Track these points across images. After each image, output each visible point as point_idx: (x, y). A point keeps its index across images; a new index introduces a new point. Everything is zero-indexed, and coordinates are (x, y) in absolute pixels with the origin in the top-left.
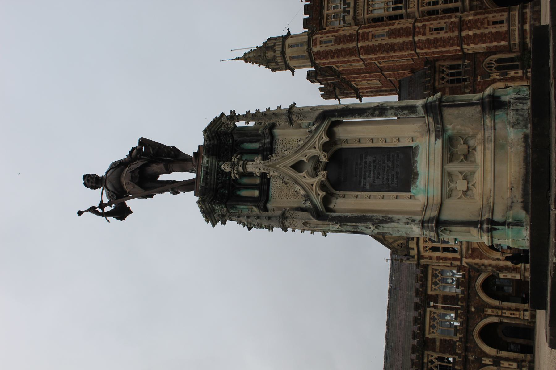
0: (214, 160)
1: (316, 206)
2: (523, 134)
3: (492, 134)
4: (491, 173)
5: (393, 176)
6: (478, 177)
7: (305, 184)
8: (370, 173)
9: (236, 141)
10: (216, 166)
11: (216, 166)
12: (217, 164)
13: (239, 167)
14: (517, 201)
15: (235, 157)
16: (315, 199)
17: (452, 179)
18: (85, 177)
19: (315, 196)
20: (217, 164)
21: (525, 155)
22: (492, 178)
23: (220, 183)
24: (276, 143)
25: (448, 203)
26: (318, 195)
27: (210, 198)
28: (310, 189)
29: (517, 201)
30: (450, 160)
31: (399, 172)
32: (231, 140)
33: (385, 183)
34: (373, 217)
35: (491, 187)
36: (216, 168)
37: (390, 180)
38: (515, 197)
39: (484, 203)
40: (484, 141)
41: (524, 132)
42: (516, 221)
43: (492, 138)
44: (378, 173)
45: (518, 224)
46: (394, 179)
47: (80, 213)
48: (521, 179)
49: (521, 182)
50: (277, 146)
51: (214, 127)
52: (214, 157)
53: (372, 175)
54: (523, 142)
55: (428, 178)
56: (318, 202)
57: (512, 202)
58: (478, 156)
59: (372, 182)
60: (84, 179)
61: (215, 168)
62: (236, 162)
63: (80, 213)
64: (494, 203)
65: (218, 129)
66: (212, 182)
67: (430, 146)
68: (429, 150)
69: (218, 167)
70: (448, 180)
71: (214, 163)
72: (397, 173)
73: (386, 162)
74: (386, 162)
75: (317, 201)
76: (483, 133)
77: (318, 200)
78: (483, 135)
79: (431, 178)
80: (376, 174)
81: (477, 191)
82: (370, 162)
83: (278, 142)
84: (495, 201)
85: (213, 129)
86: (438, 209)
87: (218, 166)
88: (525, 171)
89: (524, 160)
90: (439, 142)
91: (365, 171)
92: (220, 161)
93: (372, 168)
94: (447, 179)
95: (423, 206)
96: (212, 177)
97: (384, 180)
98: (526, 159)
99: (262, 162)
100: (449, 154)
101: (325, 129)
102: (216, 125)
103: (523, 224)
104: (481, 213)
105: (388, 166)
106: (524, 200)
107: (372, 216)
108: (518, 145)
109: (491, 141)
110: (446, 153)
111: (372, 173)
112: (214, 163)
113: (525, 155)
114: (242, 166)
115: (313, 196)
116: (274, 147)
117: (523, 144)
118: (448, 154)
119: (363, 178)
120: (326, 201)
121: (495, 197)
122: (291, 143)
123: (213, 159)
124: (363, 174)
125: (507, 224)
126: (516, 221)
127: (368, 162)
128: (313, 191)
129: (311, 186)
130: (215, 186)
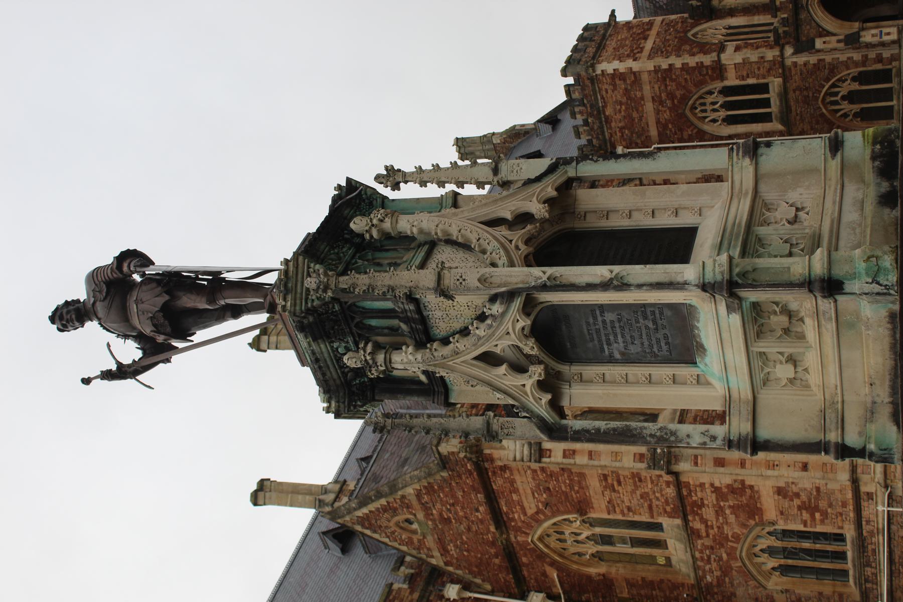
0: (322, 346)
1: (542, 417)
2: (887, 312)
3: (831, 309)
4: (835, 365)
5: (658, 341)
6: (811, 359)
7: (511, 389)
8: (616, 336)
9: (346, 303)
10: (330, 351)
11: (330, 351)
12: (329, 348)
13: (379, 367)
14: (883, 402)
15: (365, 351)
16: (537, 408)
17: (767, 358)
18: (52, 319)
19: (535, 403)
20: (329, 348)
21: (893, 341)
22: (837, 370)
23: (348, 372)
24: (428, 309)
25: (767, 397)
26: (539, 400)
27: (344, 403)
28: (521, 393)
29: (883, 402)
30: (759, 335)
31: (669, 335)
32: (335, 304)
33: (647, 351)
34: (644, 431)
35: (838, 437)
36: (332, 354)
37: (655, 346)
38: (878, 395)
39: (826, 398)
40: (817, 315)
41: (890, 309)
42: (881, 450)
43: (831, 315)
44: (631, 337)
45: (885, 458)
46: (663, 344)
47: (86, 381)
48: (887, 373)
49: (888, 377)
50: (430, 313)
51: (298, 302)
52: (320, 341)
53: (620, 339)
54: (888, 323)
55: (725, 363)
56: (544, 412)
57: (874, 403)
58: (809, 328)
59: (623, 350)
60: (53, 322)
61: (330, 354)
62: (371, 362)
63: (86, 381)
64: (843, 402)
65: (306, 303)
66: (335, 376)
67: (720, 319)
68: (718, 323)
69: (333, 351)
70: (760, 364)
71: (324, 349)
72: (666, 337)
73: (641, 320)
74: (641, 320)
75: (540, 411)
76: (814, 303)
77: (542, 408)
78: (815, 306)
79: (730, 364)
80: (628, 337)
81: (814, 379)
82: (612, 322)
83: (430, 307)
84: (845, 398)
85: (298, 308)
86: (750, 417)
87: (332, 350)
88: (893, 362)
89: (891, 348)
90: (735, 319)
91: (607, 335)
92: (333, 342)
93: (618, 330)
94: (757, 363)
95: (723, 400)
96: (332, 369)
97: (645, 346)
98: (893, 347)
99: (419, 356)
100: (755, 327)
101: (518, 310)
102: (298, 295)
103: (893, 458)
104: (823, 422)
105: (647, 327)
106: (893, 401)
107: (641, 428)
108: (880, 326)
109: (830, 319)
110: (751, 328)
111: (619, 336)
112: (324, 349)
113: (893, 341)
114: (383, 365)
115: (531, 405)
116: (425, 313)
117: (889, 326)
118: (754, 328)
119: (605, 343)
120: (556, 405)
121: (845, 393)
122: (455, 308)
123: (319, 345)
124: (604, 338)
125: (867, 454)
126: (881, 450)
127: (608, 321)
128: (528, 396)
129: (522, 387)
130: (342, 379)
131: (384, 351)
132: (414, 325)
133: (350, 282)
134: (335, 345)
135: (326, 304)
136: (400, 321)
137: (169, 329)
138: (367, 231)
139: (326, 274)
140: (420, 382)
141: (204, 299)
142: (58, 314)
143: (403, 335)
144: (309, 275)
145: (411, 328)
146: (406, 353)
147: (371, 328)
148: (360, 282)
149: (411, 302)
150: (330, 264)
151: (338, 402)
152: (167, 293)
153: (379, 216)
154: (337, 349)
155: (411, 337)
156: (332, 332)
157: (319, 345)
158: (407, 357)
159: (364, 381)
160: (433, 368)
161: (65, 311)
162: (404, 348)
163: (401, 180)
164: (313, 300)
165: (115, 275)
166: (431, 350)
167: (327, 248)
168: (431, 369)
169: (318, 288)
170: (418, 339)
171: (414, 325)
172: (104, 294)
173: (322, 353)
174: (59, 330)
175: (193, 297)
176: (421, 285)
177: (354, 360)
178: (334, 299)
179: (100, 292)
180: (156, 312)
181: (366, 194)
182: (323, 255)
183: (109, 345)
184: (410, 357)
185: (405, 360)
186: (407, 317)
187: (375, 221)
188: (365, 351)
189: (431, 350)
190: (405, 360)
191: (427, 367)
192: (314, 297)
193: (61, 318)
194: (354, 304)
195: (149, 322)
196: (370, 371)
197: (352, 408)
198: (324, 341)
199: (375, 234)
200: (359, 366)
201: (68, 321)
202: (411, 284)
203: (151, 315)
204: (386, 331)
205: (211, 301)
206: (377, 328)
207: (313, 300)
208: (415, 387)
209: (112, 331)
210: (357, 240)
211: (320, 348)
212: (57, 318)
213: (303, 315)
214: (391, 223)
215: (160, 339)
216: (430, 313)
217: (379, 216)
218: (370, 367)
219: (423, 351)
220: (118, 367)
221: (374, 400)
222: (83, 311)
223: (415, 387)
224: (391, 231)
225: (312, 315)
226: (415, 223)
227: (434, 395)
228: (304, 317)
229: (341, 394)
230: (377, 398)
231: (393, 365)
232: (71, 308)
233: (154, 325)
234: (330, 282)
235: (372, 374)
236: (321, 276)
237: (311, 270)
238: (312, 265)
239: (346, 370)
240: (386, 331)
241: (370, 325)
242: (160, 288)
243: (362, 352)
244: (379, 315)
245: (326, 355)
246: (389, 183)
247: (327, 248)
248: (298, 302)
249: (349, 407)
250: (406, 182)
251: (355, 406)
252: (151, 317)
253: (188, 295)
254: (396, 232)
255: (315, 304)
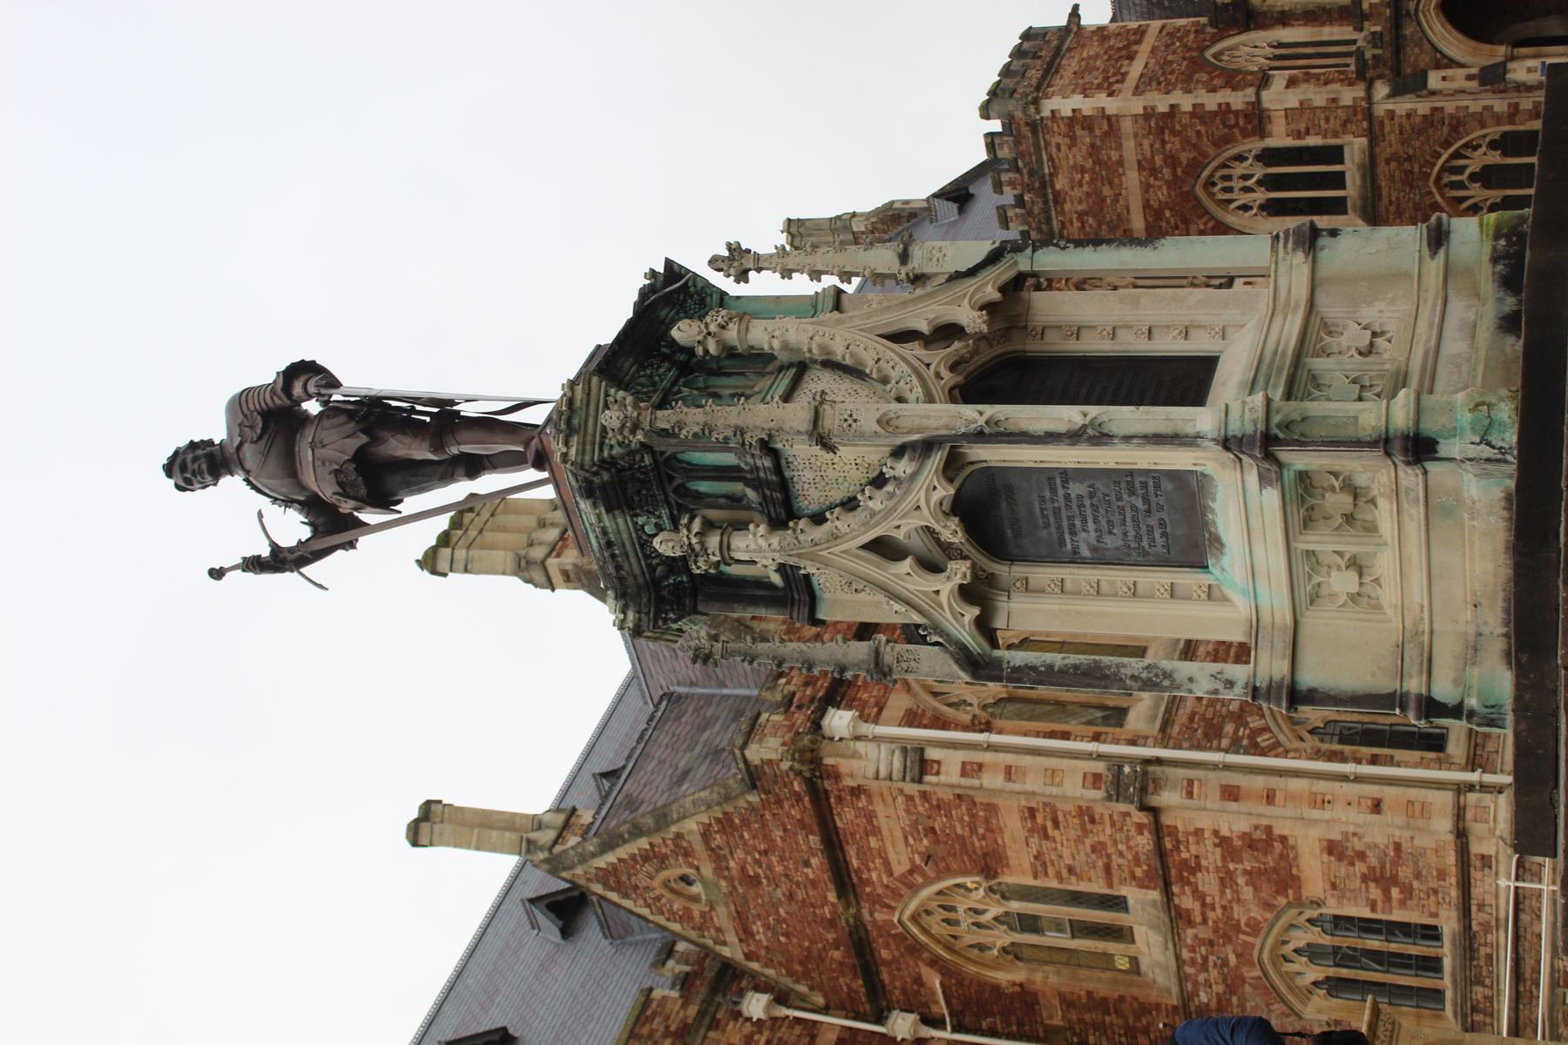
0: (620, 521)
5: (1150, 530)
6: (1385, 564)
8: (1084, 520)
9: (662, 453)
15: (689, 531)
23: (658, 565)
25: (1314, 622)
27: (648, 614)
30: (1307, 523)
37: (1145, 538)
38: (1485, 623)
44: (1108, 522)
45: (1493, 720)
46: (1157, 535)
47: (217, 574)
48: (1500, 588)
50: (796, 473)
51: (588, 448)
52: (616, 512)
53: (1091, 526)
54: (1504, 508)
58: (1384, 515)
62: (697, 547)
63: (217, 574)
64: (1432, 632)
65: (601, 450)
66: (637, 571)
67: (1248, 495)
68: (1245, 503)
69: (636, 530)
70: (1307, 569)
71: (622, 527)
72: (1162, 524)
73: (1125, 496)
74: (1125, 496)
76: (1393, 475)
80: (1104, 523)
81: (1388, 595)
82: (1080, 497)
84: (1435, 626)
85: (587, 458)
86: (1289, 652)
90: (1272, 496)
91: (1070, 518)
92: (637, 515)
93: (1089, 511)
94: (1302, 568)
95: (1248, 625)
96: (633, 559)
99: (775, 541)
101: (936, 471)
102: (589, 438)
105: (1134, 508)
107: (1117, 666)
108: (1490, 514)
109: (1416, 501)
110: (1295, 511)
111: (1090, 521)
112: (622, 527)
114: (717, 553)
116: (787, 474)
119: (1066, 531)
120: (984, 625)
121: (1435, 618)
123: (615, 519)
124: (1065, 523)
127: (1073, 496)
128: (943, 609)
129: (934, 595)
131: (719, 531)
132: (768, 493)
133: (674, 419)
134: (641, 520)
135: (631, 453)
136: (747, 485)
137: (363, 492)
138: (699, 342)
139: (636, 406)
140: (771, 586)
141: (426, 444)
142: (179, 461)
143: (749, 508)
144: (607, 407)
145: (764, 496)
146: (754, 535)
147: (698, 496)
148: (689, 420)
149: (767, 455)
150: (638, 392)
151: (639, 612)
152: (364, 431)
153: (720, 320)
154: (643, 527)
155: (762, 512)
156: (636, 499)
157: (615, 519)
158: (756, 542)
159: (682, 582)
160: (796, 560)
161: (190, 457)
162: (751, 527)
163: (751, 266)
164: (611, 447)
165: (278, 401)
166: (794, 531)
167: (634, 368)
168: (792, 561)
169: (623, 426)
170: (773, 515)
171: (768, 493)
172: (259, 431)
173: (619, 532)
174: (179, 487)
175: (407, 440)
176: (786, 427)
177: (671, 544)
178: (644, 447)
179: (252, 427)
180: (345, 462)
181: (695, 286)
182: (627, 378)
183: (260, 515)
184: (762, 542)
185: (753, 546)
186: (759, 478)
187: (713, 328)
188: (689, 531)
189: (794, 531)
190: (753, 546)
191: (787, 558)
192: (613, 442)
193: (183, 469)
194: (674, 457)
195: (332, 478)
196: (696, 562)
197: (660, 622)
198: (623, 512)
199: (712, 348)
200: (679, 554)
201: (194, 474)
202: (772, 425)
203: (336, 467)
204: (722, 501)
205: (438, 447)
206: (709, 496)
207: (611, 447)
208: (762, 593)
209: (267, 491)
210: (681, 357)
211: (617, 524)
212: (176, 468)
213: (595, 469)
214: (739, 331)
215: (346, 507)
216: (796, 473)
217: (720, 320)
218: (697, 556)
219: (781, 532)
220: (273, 552)
221: (695, 612)
222: (219, 458)
223: (762, 593)
224: (737, 343)
225: (608, 470)
226: (776, 334)
227: (792, 606)
228: (596, 474)
229: (644, 600)
230: (700, 608)
231: (734, 554)
232: (200, 452)
233: (340, 484)
234: (641, 418)
235: (698, 568)
236: (629, 408)
237: (611, 399)
238: (612, 391)
239: (655, 562)
240: (722, 501)
241: (696, 491)
242: (352, 425)
243: (684, 531)
244: (714, 474)
245: (625, 536)
246: (732, 271)
247: (634, 368)
248: (588, 448)
249: (656, 622)
250: (759, 270)
251: (665, 621)
252: (336, 470)
253: (399, 437)
254: (745, 346)
255: (614, 452)
